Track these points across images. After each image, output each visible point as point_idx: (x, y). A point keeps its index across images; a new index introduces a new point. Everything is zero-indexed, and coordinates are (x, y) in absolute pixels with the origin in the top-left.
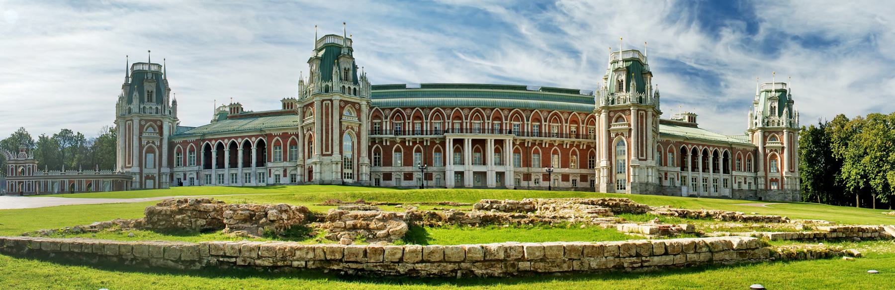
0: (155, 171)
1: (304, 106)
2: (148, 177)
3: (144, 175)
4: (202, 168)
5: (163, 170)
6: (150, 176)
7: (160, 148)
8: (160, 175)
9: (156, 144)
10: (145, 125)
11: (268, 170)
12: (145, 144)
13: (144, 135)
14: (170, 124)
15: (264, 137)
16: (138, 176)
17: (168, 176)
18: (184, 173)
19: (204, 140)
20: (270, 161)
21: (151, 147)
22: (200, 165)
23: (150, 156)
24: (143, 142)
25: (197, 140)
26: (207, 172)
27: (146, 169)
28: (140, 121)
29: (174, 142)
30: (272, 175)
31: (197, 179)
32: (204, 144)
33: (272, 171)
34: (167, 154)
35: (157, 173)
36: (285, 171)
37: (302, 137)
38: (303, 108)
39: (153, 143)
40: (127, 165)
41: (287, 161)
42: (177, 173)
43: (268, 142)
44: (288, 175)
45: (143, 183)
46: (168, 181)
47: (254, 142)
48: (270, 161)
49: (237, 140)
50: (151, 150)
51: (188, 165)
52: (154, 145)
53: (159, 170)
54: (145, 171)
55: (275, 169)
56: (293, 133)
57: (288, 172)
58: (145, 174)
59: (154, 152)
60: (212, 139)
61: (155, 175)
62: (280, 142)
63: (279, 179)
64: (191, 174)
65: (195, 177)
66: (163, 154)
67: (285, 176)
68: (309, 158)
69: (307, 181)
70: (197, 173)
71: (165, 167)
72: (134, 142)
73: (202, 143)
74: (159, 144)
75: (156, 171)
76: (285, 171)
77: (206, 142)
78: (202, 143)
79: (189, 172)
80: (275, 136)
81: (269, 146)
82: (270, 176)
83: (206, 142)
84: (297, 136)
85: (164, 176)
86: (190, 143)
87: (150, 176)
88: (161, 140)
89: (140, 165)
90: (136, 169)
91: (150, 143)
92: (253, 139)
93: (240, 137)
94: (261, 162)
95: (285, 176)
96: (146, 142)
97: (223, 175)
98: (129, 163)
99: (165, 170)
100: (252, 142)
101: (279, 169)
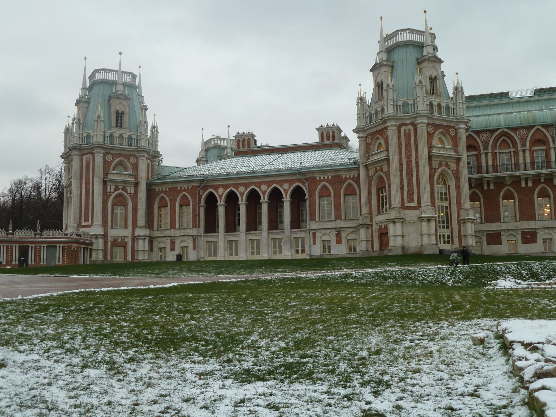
0: (127, 233)
1: (368, 135)
2: (115, 243)
3: (110, 240)
4: (202, 232)
5: (139, 232)
6: (119, 240)
7: (135, 196)
8: (135, 239)
9: (129, 192)
10: (112, 162)
11: (311, 233)
12: (112, 190)
13: (110, 177)
14: (149, 161)
15: (304, 183)
16: (101, 241)
17: (147, 241)
18: (171, 240)
19: (205, 188)
20: (313, 219)
21: (120, 195)
22: (199, 226)
23: (119, 210)
24: (109, 187)
25: (193, 187)
26: (211, 237)
27: (112, 230)
28: (105, 155)
29: (155, 190)
30: (318, 241)
31: (194, 248)
32: (206, 194)
33: (318, 235)
34: (144, 207)
35: (130, 236)
36: (338, 235)
37: (367, 182)
38: (366, 137)
39: (124, 189)
40: (83, 223)
41: (341, 220)
42: (160, 240)
43: (310, 191)
44: (343, 241)
45: (109, 252)
46: (147, 249)
47: (288, 190)
48: (313, 219)
49: (259, 187)
50: (120, 201)
51: (177, 226)
52: (125, 193)
53: (133, 232)
54: (112, 233)
55: (323, 232)
56: (350, 176)
57: (343, 235)
58: (111, 237)
59: (125, 205)
60: (219, 186)
61: (126, 240)
62: (329, 189)
63: (329, 247)
64: (184, 241)
65: (191, 245)
66: (139, 207)
67: (339, 242)
68: (379, 213)
69: (378, 249)
70: (194, 240)
71: (141, 227)
72: (95, 187)
73: (201, 192)
74: (132, 192)
75: (127, 233)
76: (338, 235)
77: (208, 191)
78: (201, 192)
79: (181, 238)
80: (321, 181)
81: (312, 196)
82: (314, 244)
83: (208, 191)
84: (357, 180)
85: (141, 242)
86: (181, 191)
87: (119, 240)
88: (136, 185)
89: (104, 223)
90: (97, 230)
91: (119, 189)
92: (286, 186)
93: (265, 183)
94: (297, 223)
95: (339, 242)
96: (113, 187)
97: (236, 241)
98: (86, 220)
99: (141, 232)
100: (284, 190)
101: (329, 231)
